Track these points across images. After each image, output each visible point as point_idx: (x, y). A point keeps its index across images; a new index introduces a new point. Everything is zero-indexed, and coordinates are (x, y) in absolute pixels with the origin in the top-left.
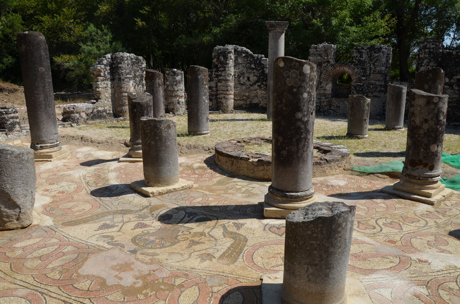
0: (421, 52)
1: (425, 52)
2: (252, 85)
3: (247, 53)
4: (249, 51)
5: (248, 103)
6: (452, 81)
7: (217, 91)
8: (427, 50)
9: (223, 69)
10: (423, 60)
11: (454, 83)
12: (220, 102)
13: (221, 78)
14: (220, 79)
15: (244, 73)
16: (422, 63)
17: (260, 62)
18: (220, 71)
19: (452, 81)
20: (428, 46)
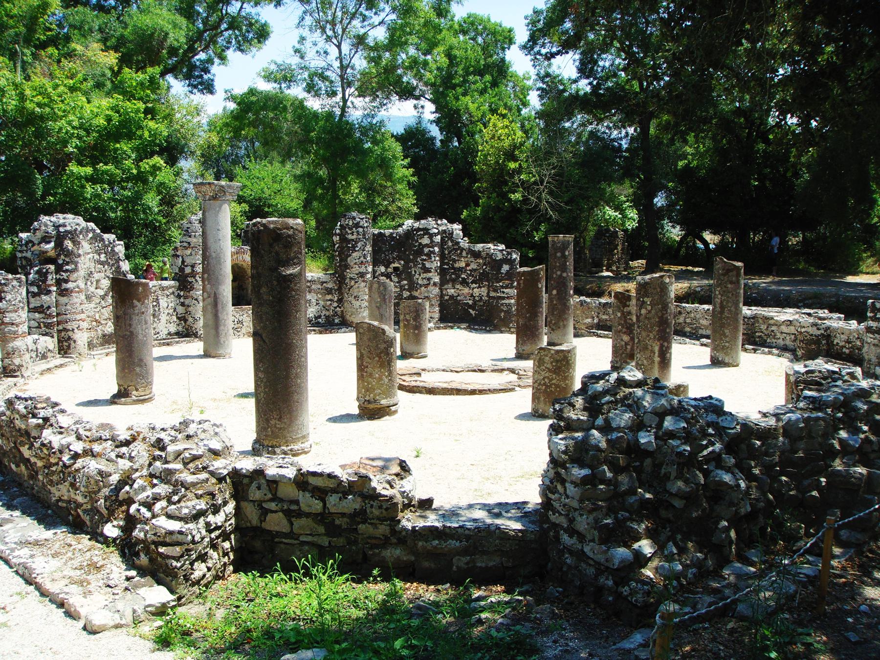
0: (349, 232)
1: (358, 232)
2: (103, 298)
3: (93, 231)
4: (96, 228)
5: (100, 333)
6: (390, 270)
7: (58, 315)
8: (361, 230)
9: (73, 266)
10: (356, 243)
11: (392, 273)
12: (69, 338)
13: (70, 285)
14: (66, 290)
15: (91, 272)
16: (354, 247)
17: (113, 250)
18: (67, 271)
19: (390, 270)
20: (361, 224)
